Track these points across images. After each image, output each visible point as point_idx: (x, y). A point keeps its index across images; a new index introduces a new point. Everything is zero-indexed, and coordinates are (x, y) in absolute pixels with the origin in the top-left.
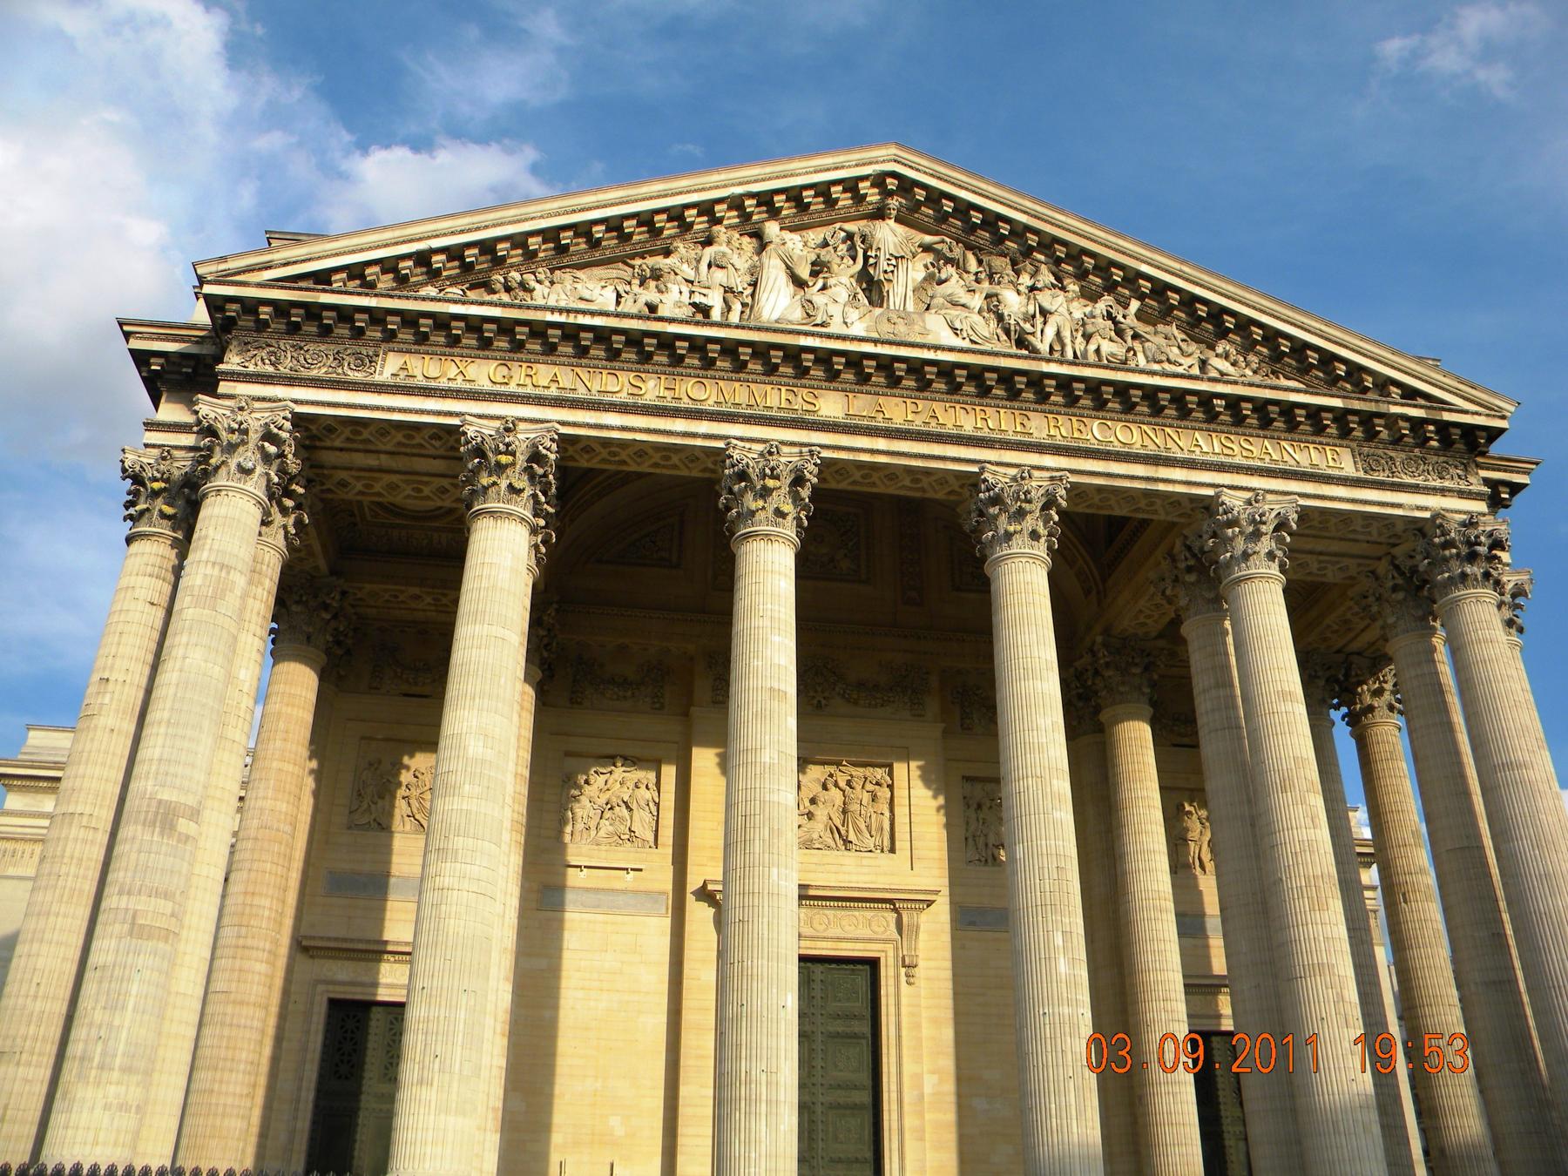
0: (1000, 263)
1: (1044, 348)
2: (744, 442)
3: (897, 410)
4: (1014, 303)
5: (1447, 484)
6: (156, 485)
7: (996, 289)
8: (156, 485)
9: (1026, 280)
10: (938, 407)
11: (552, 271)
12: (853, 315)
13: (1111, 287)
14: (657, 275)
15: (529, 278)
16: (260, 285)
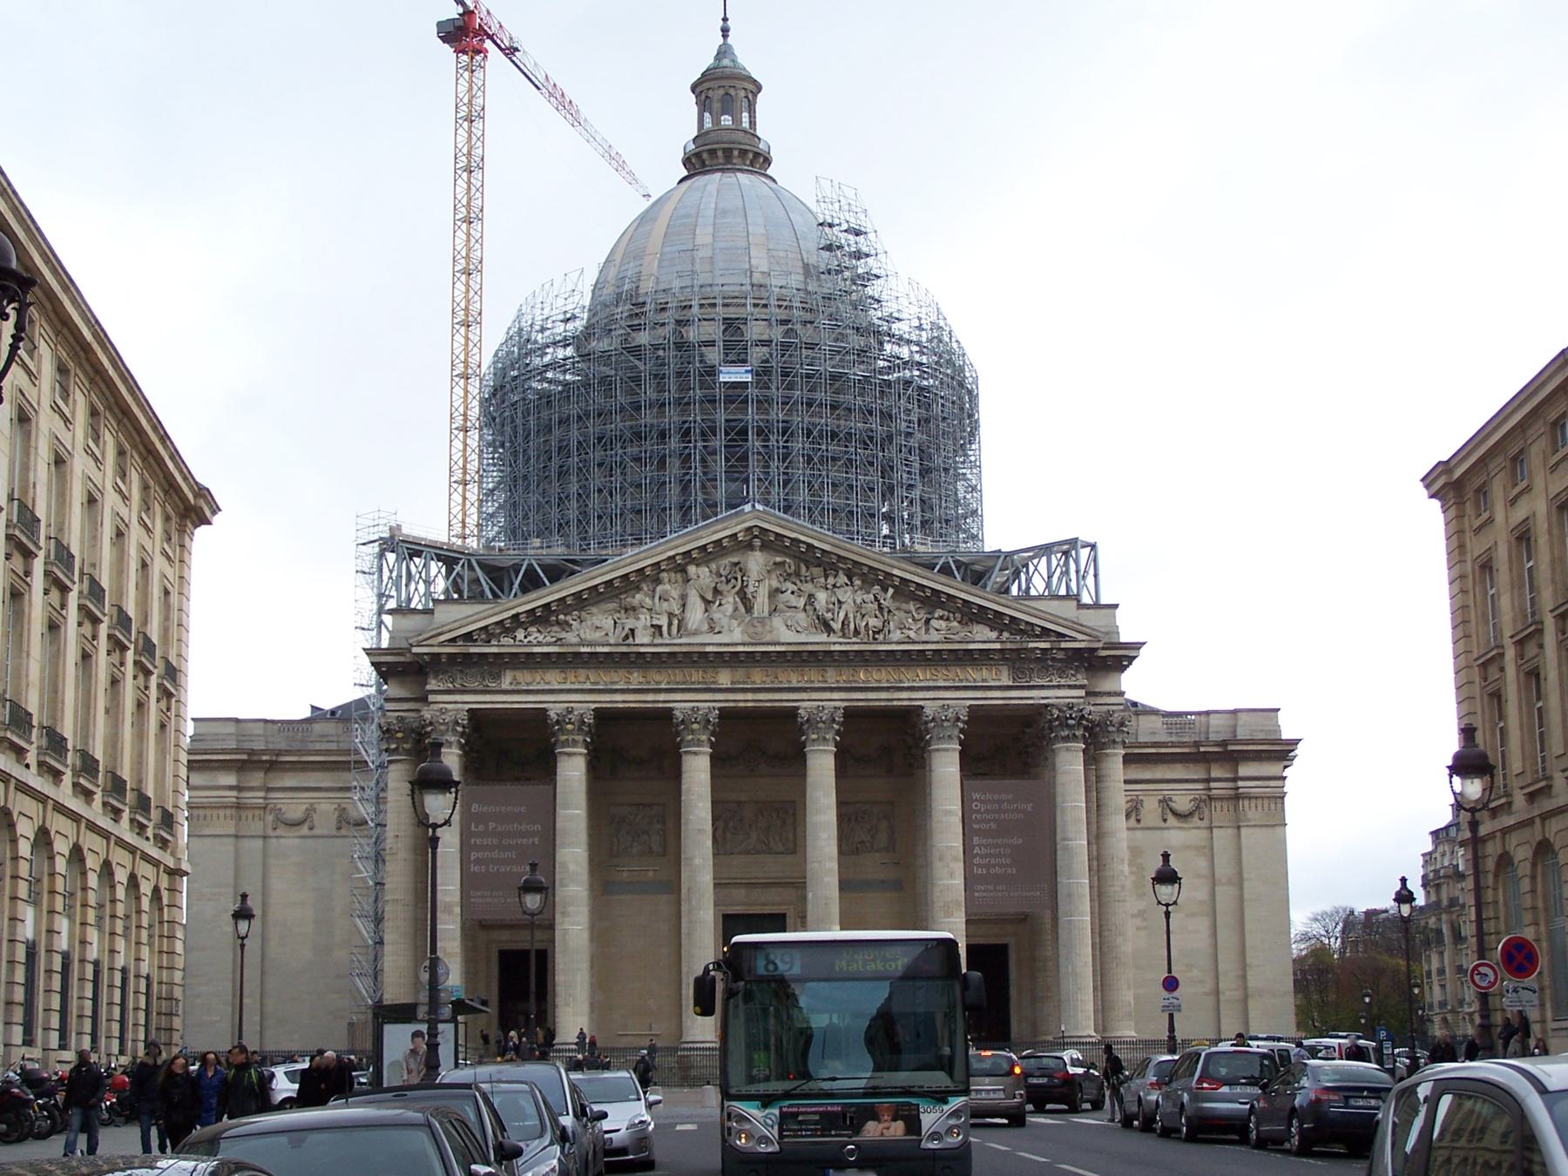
0: (817, 571)
1: (836, 626)
2: (681, 703)
3: (758, 677)
4: (822, 597)
5: (1063, 682)
6: (400, 735)
7: (813, 591)
8: (400, 735)
9: (831, 580)
10: (779, 670)
11: (580, 610)
12: (735, 623)
13: (879, 582)
14: (634, 609)
15: (569, 618)
16: (441, 644)
